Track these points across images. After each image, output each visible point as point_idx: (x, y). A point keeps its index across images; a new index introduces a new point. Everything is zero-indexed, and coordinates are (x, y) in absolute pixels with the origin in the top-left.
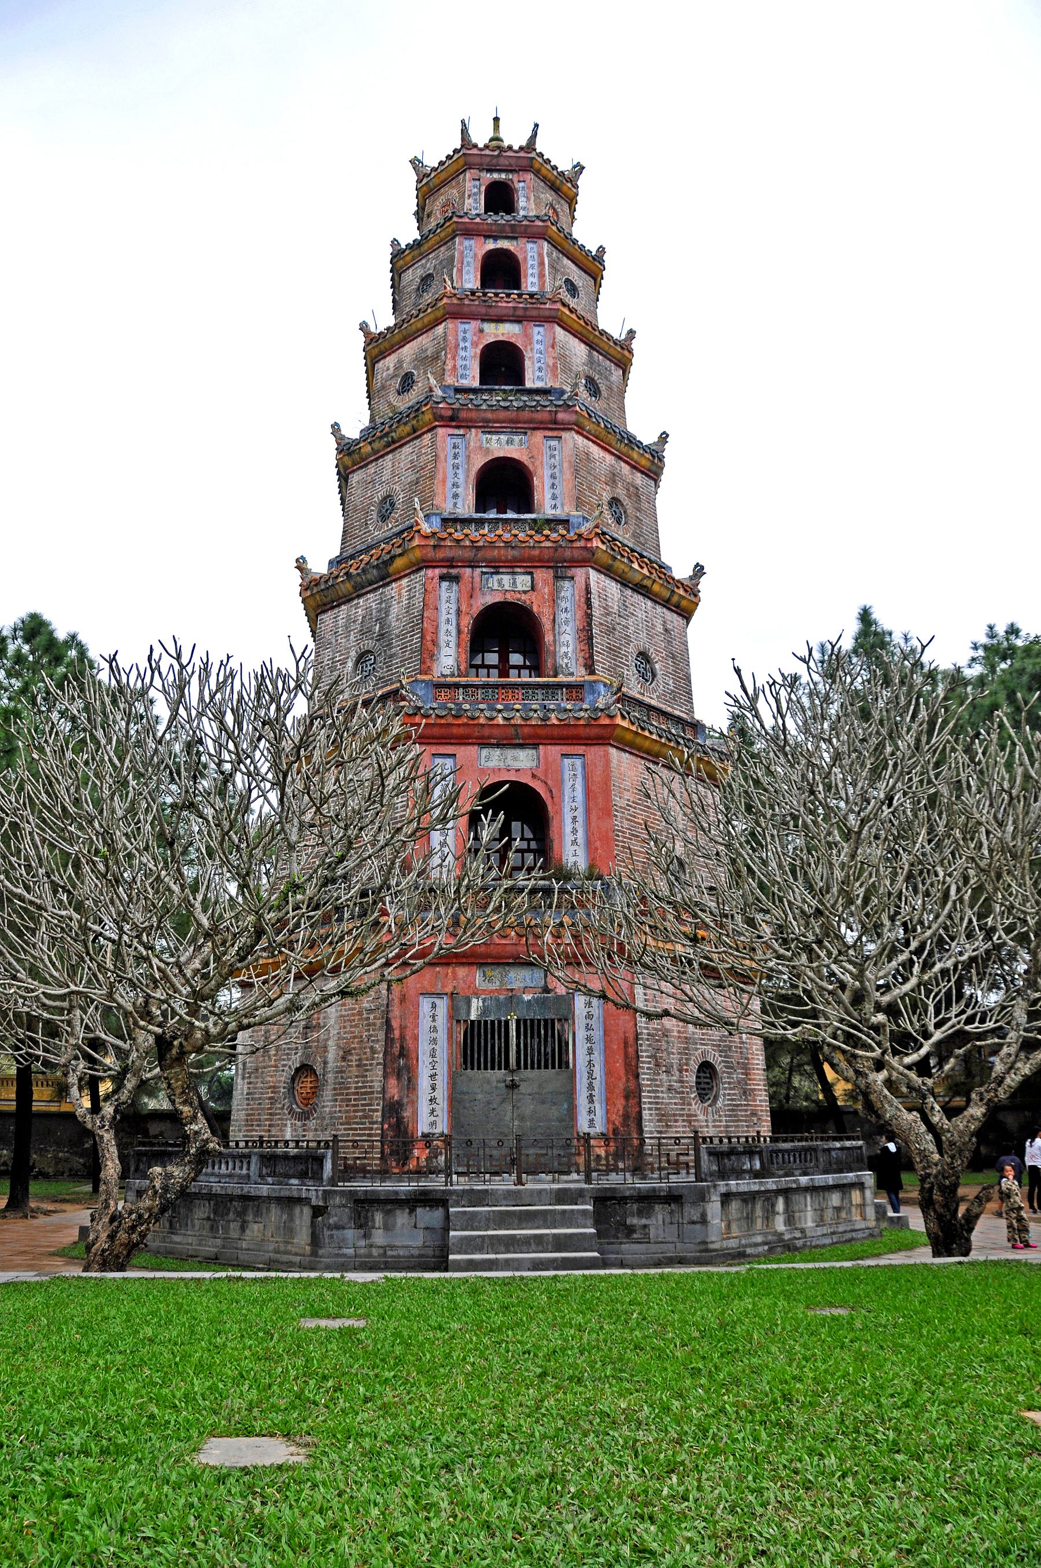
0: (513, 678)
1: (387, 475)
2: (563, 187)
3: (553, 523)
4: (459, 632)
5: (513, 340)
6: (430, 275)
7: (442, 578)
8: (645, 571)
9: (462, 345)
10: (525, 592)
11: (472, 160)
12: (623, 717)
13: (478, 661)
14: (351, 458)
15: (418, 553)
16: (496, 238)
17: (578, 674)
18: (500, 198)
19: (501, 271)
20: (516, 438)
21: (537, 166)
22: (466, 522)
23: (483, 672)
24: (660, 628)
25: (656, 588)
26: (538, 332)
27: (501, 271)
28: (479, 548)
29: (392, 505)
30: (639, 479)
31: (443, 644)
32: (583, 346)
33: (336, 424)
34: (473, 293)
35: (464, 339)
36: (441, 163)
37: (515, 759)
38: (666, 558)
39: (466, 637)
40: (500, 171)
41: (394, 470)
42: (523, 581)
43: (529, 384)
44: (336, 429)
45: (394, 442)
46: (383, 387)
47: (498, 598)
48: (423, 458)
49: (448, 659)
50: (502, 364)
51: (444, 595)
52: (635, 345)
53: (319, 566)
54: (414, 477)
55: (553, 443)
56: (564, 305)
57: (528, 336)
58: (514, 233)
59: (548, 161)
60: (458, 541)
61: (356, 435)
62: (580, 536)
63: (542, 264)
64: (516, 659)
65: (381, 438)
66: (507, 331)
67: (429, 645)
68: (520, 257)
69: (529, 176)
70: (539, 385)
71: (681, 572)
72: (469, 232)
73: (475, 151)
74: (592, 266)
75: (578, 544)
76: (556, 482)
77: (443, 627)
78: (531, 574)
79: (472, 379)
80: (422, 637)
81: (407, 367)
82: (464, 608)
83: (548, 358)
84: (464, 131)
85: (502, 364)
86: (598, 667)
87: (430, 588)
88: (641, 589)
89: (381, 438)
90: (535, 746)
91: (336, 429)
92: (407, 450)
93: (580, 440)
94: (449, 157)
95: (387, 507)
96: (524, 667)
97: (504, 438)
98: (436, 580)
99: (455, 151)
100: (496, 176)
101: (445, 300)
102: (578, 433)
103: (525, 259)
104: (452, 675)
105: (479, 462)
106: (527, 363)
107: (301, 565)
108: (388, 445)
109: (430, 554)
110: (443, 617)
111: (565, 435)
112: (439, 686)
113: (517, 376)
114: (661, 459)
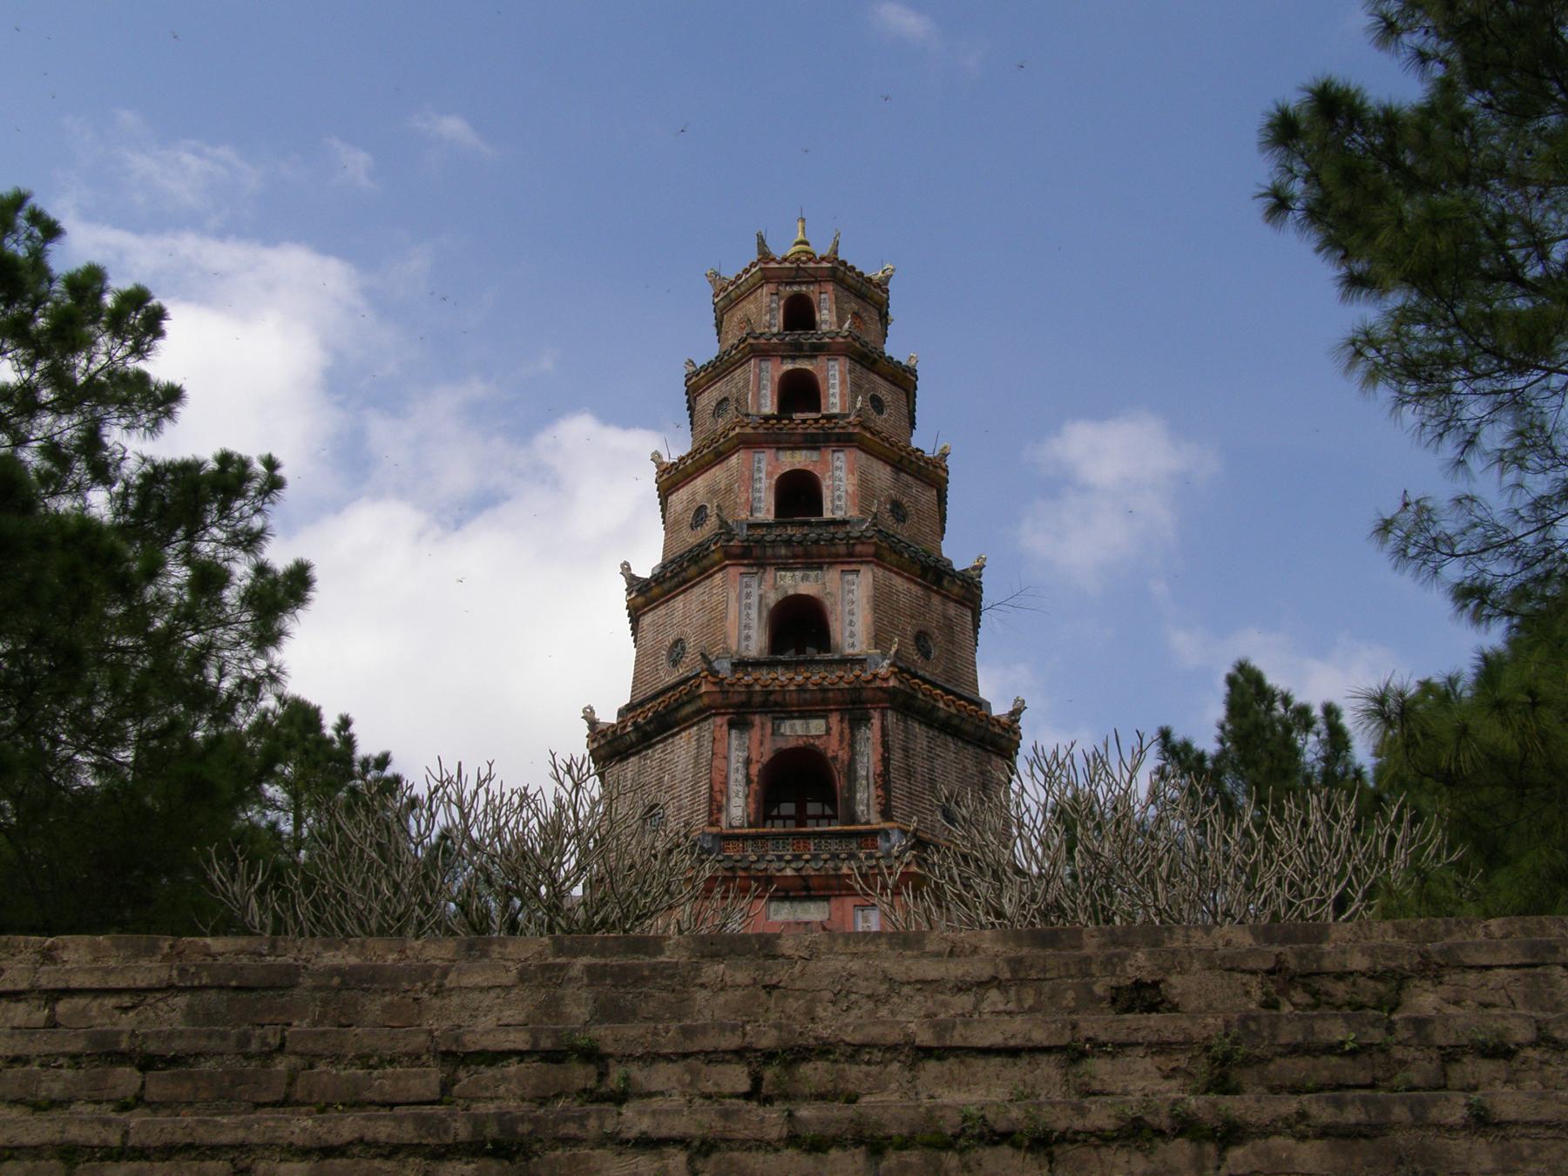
0: (811, 828)
1: (678, 614)
4: (749, 781)
5: (810, 468)
6: (726, 399)
7: (732, 725)
8: (953, 710)
9: (757, 476)
10: (819, 737)
11: (768, 274)
12: (919, 865)
13: (775, 813)
14: (645, 597)
15: (706, 700)
16: (793, 358)
17: (876, 822)
18: (799, 314)
19: (800, 392)
20: (812, 574)
21: (840, 274)
22: (757, 664)
23: (779, 823)
24: (972, 770)
25: (968, 727)
27: (800, 392)
28: (771, 693)
29: (683, 648)
30: (952, 609)
31: (732, 795)
32: (889, 469)
33: (626, 563)
34: (767, 418)
35: (759, 470)
36: (739, 277)
37: (806, 912)
38: (985, 691)
39: (754, 786)
40: (800, 283)
41: (685, 611)
42: (817, 726)
43: (827, 515)
44: (626, 568)
45: (685, 581)
46: (676, 522)
47: (791, 744)
48: (715, 598)
49: (738, 809)
50: (799, 494)
51: (734, 743)
52: (949, 462)
53: (608, 715)
54: (705, 619)
55: (850, 577)
56: (865, 428)
57: (824, 462)
58: (817, 350)
59: (853, 269)
60: (748, 686)
61: (647, 575)
62: (875, 676)
63: (843, 382)
64: (813, 808)
65: (672, 578)
67: (718, 796)
68: (820, 377)
69: (830, 287)
70: (839, 515)
71: (1000, 709)
72: (762, 352)
73: (773, 265)
75: (873, 685)
76: (854, 618)
77: (733, 777)
78: (825, 717)
79: (766, 511)
80: (711, 788)
81: (700, 499)
82: (754, 756)
84: (761, 242)
85: (799, 494)
86: (897, 814)
87: (718, 736)
88: (948, 728)
89: (672, 578)
90: (826, 898)
91: (626, 568)
92: (697, 591)
93: (880, 572)
94: (746, 271)
95: (677, 650)
96: (823, 817)
97: (799, 574)
98: (725, 728)
99: (753, 265)
100: (796, 288)
101: (738, 430)
102: (878, 565)
103: (826, 379)
104: (742, 827)
105: (773, 598)
106: (826, 494)
107: (589, 716)
108: (678, 586)
109: (719, 699)
110: (733, 765)
111: (863, 568)
112: (727, 838)
113: (817, 508)
114: (979, 586)
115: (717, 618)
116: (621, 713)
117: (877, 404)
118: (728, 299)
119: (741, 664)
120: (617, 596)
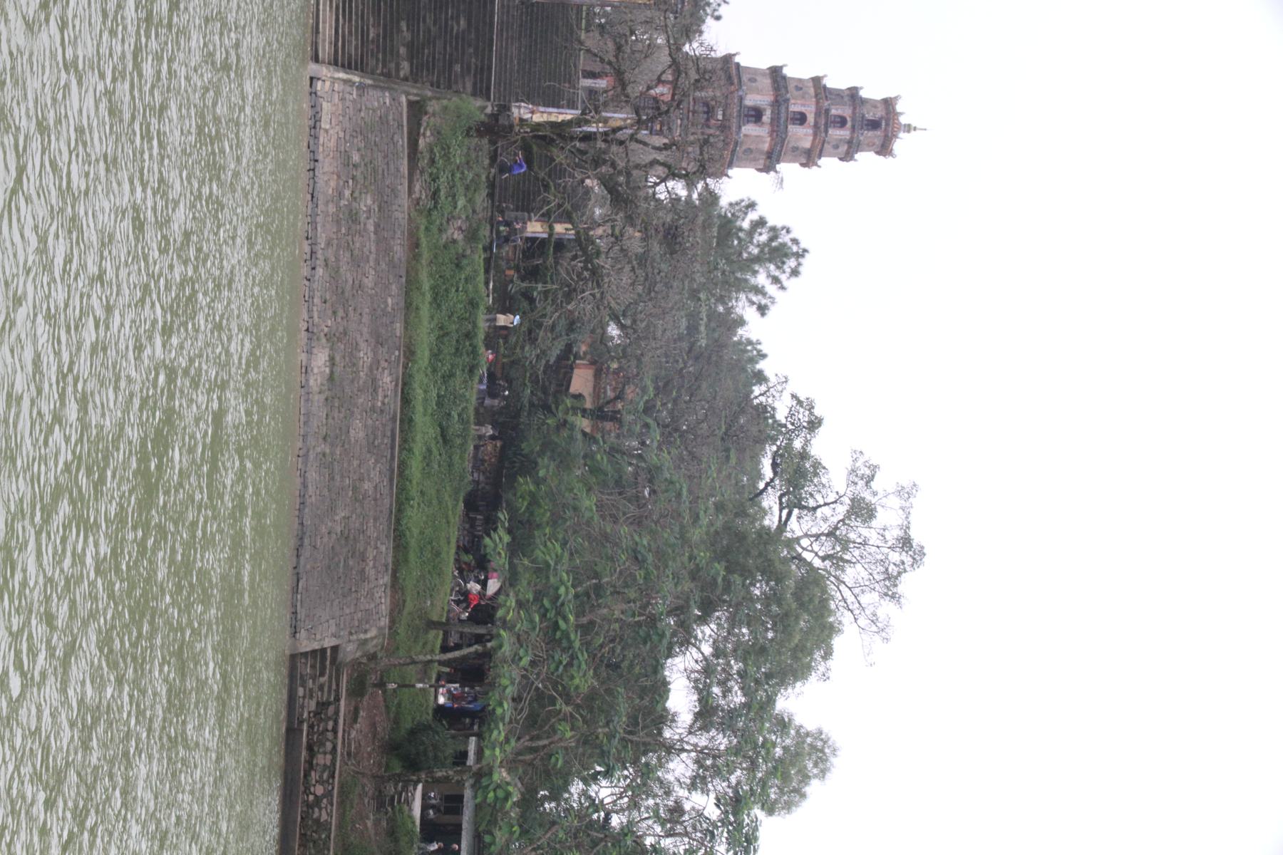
2: (884, 149)
3: (740, 128)
18: (874, 125)
26: (810, 131)
27: (842, 122)
34: (827, 111)
42: (720, 117)
53: (737, 59)
66: (811, 118)
74: (847, 157)
83: (801, 136)
115: (759, 91)
116: (738, 65)
117: (836, 147)
118: (888, 103)
119: (741, 99)
120: (779, 64)
